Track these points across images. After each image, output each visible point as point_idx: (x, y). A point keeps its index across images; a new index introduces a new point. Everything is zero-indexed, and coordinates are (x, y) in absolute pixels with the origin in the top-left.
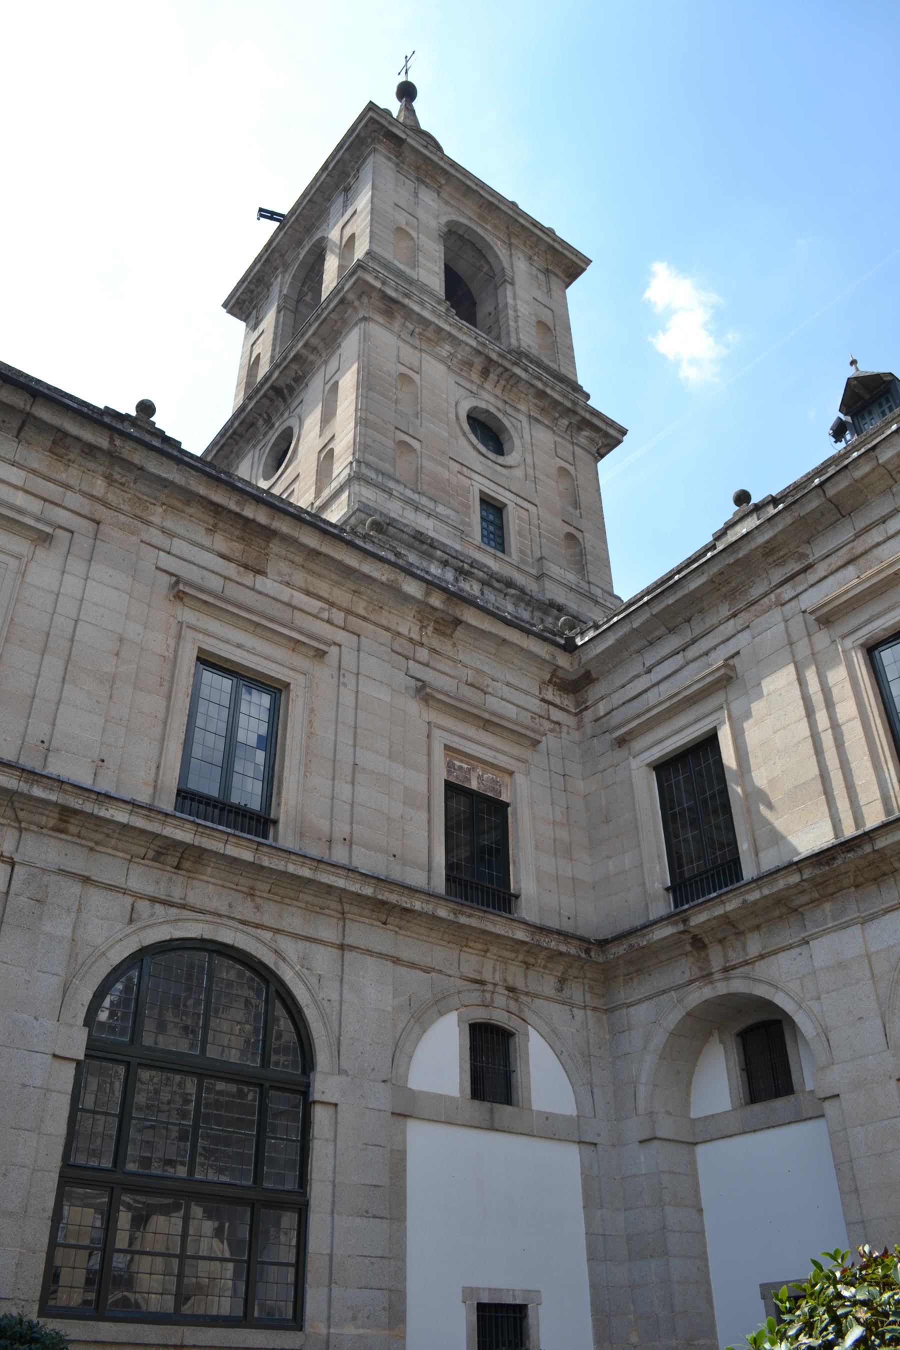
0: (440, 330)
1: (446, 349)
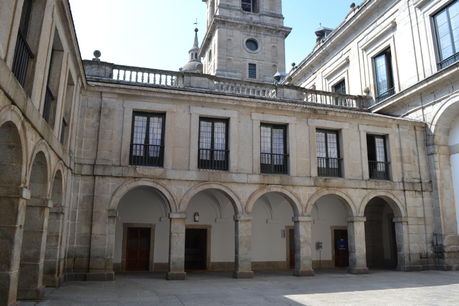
0: (237, 23)
1: (239, 26)
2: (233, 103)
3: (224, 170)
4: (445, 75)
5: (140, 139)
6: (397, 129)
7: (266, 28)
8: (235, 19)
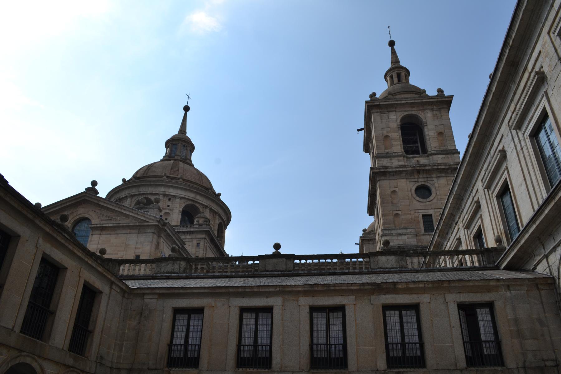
1: (404, 174)
2: (276, 288)
3: (267, 368)
4: (546, 212)
5: (179, 339)
6: (508, 293)
7: (438, 169)
8: (396, 167)
